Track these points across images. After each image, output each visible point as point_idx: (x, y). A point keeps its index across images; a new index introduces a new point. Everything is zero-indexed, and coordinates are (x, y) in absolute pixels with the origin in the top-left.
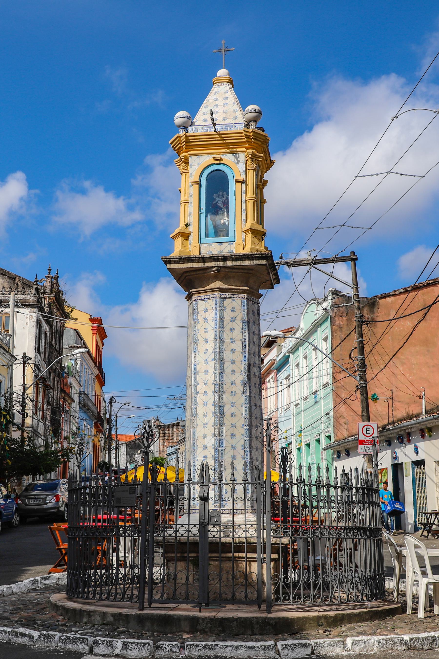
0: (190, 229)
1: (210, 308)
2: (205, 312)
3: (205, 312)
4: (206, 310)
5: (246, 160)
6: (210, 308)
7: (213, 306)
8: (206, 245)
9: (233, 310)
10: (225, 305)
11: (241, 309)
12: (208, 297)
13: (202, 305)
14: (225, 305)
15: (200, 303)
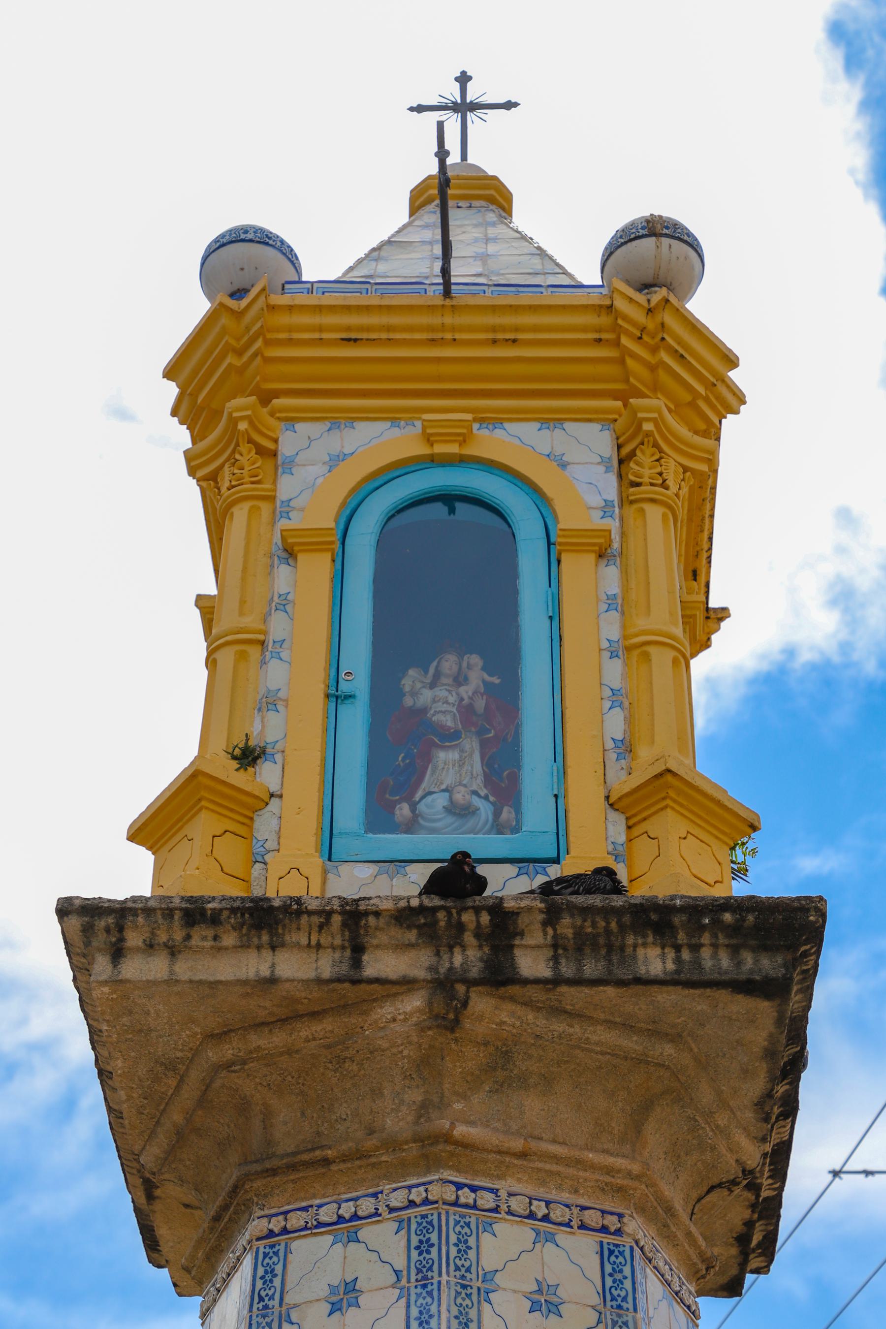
0: (267, 774)
1: (373, 1276)
2: (336, 1308)
3: (336, 1308)
4: (344, 1297)
5: (621, 462)
6: (373, 1276)
7: (400, 1263)
8: (372, 869)
9: (545, 1301)
10: (489, 1262)
11: (596, 1300)
12: (367, 1206)
13: (315, 1263)
14: (489, 1262)
15: (304, 1250)
